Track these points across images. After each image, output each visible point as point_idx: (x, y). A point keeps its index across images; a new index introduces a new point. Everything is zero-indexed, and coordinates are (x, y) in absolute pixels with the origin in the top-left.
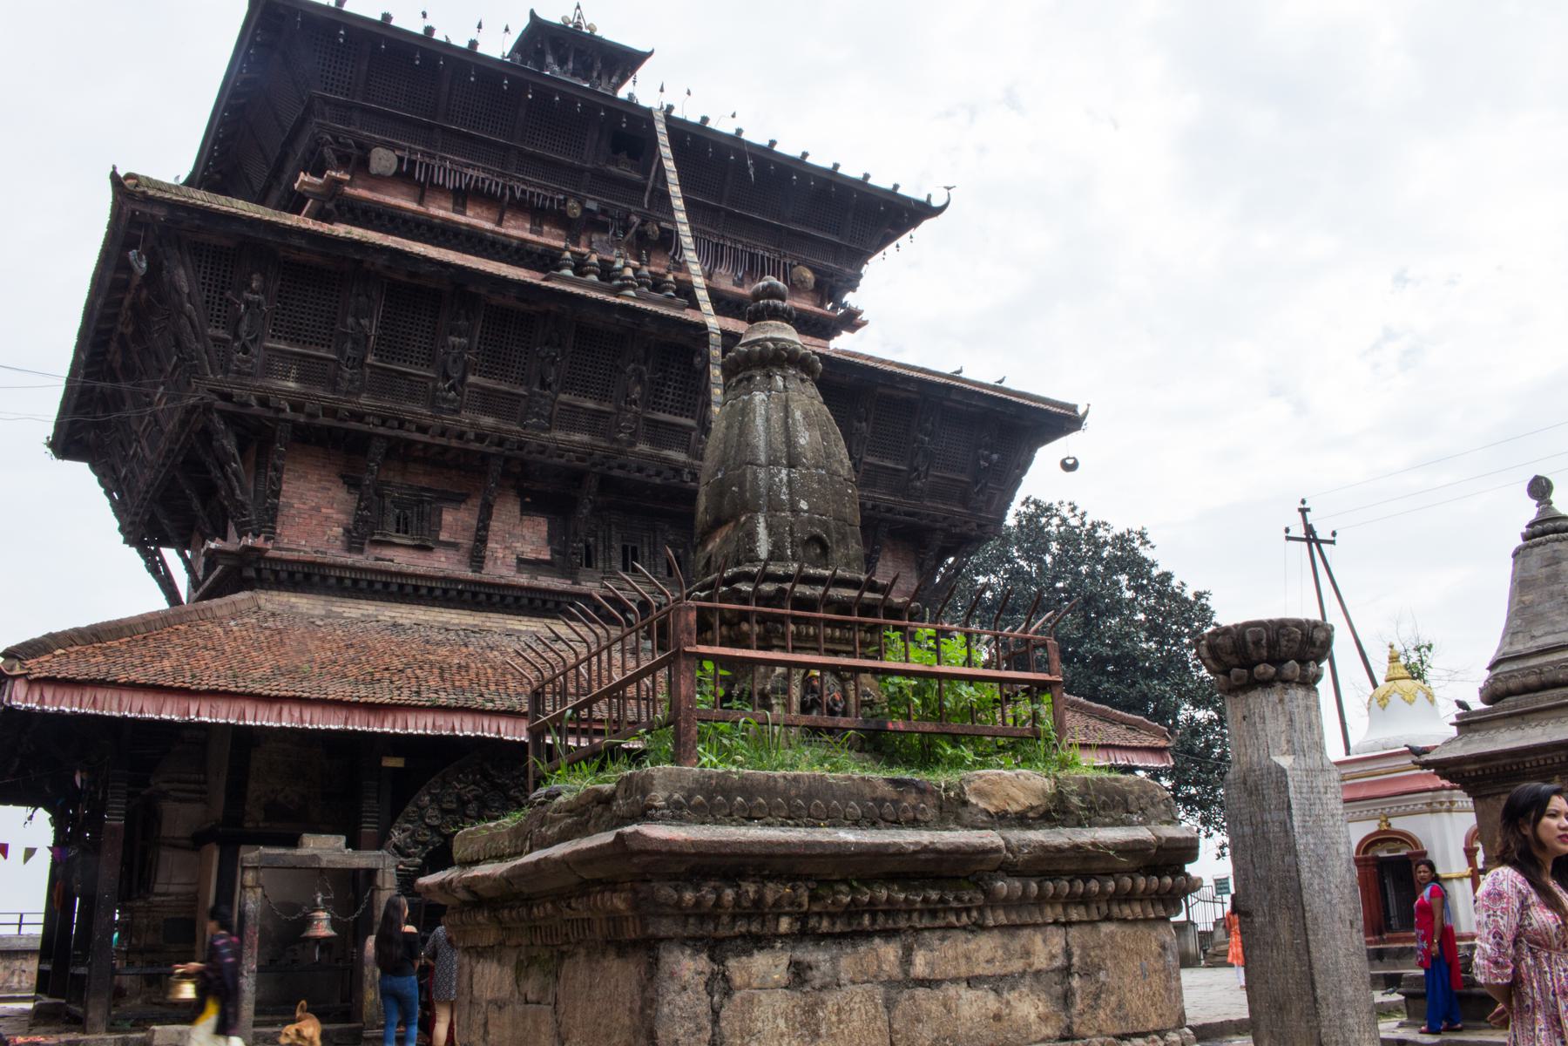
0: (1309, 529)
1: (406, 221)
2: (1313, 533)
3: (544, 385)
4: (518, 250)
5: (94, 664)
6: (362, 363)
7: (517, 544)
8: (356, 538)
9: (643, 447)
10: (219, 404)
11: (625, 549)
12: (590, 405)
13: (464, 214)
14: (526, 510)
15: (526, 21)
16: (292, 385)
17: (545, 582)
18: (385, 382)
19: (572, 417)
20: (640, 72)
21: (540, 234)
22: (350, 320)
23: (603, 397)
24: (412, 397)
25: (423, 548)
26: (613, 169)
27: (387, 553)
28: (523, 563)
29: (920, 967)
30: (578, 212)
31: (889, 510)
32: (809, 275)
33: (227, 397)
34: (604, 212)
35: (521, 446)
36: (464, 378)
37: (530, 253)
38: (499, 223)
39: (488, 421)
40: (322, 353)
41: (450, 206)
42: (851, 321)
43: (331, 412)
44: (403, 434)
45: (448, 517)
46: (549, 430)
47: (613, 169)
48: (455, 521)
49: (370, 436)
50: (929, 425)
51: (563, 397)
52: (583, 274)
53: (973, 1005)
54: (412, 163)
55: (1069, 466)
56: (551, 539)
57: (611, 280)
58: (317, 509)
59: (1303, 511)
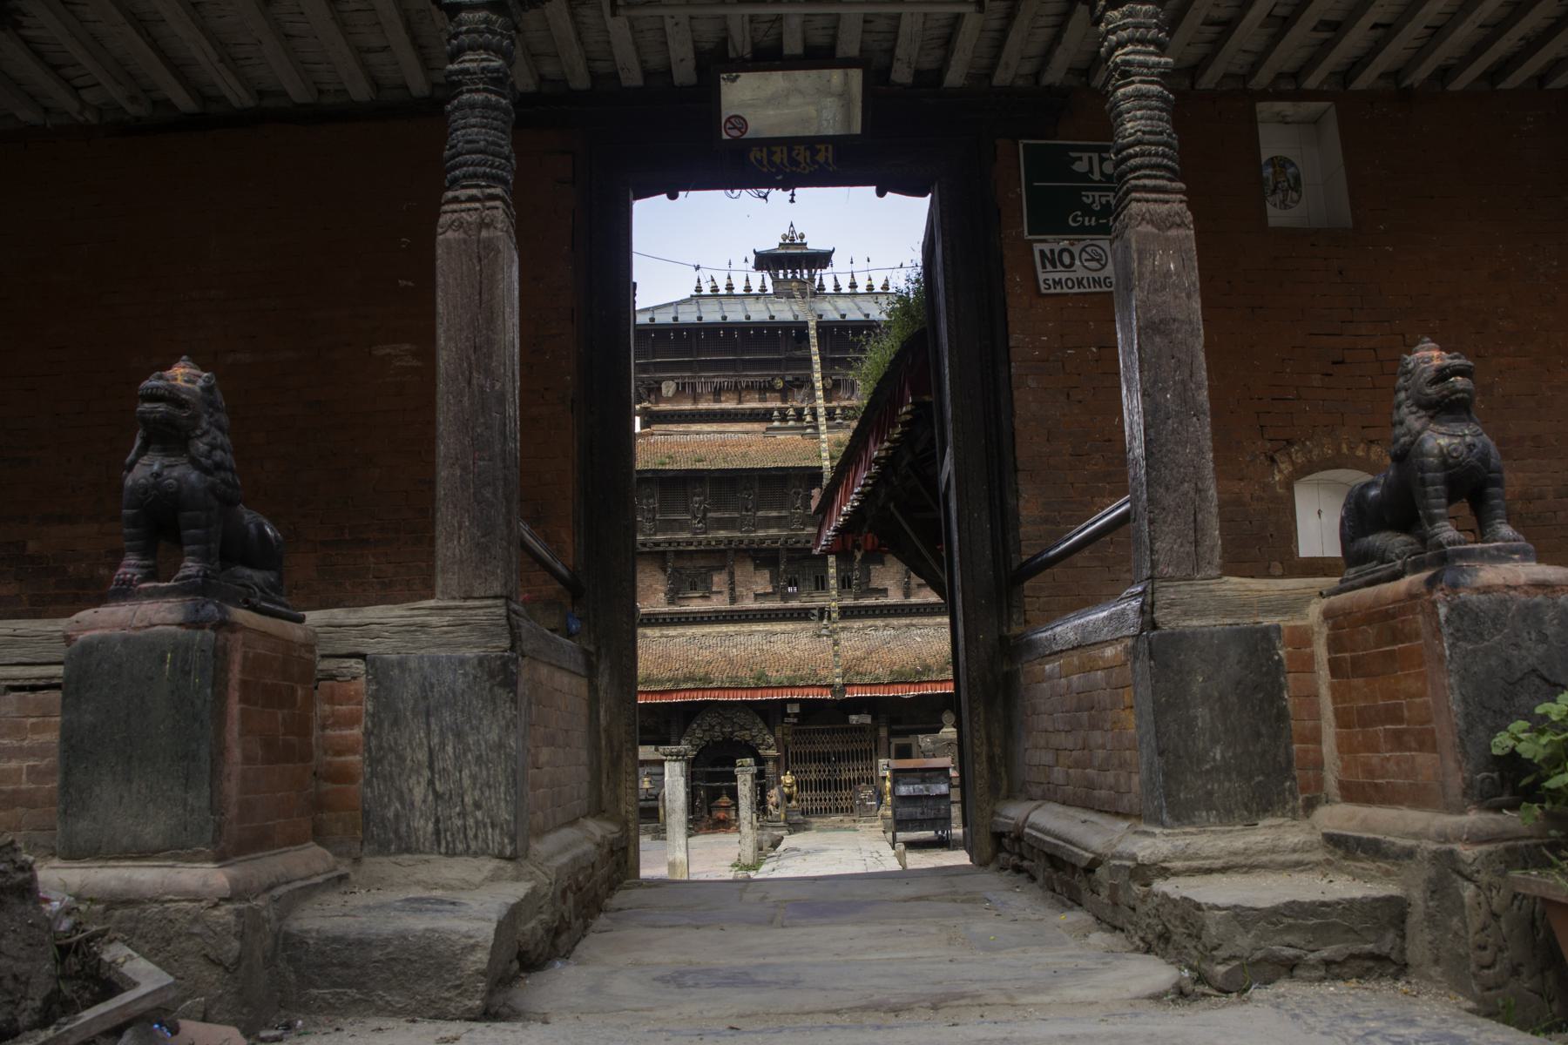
7: (755, 588)
12: (775, 514)
14: (757, 567)
17: (767, 605)
18: (669, 526)
19: (767, 523)
23: (782, 508)
24: (682, 529)
26: (798, 353)
28: (757, 596)
35: (741, 542)
39: (722, 534)
45: (716, 579)
48: (719, 580)
49: (664, 553)
51: (760, 514)
56: (774, 579)
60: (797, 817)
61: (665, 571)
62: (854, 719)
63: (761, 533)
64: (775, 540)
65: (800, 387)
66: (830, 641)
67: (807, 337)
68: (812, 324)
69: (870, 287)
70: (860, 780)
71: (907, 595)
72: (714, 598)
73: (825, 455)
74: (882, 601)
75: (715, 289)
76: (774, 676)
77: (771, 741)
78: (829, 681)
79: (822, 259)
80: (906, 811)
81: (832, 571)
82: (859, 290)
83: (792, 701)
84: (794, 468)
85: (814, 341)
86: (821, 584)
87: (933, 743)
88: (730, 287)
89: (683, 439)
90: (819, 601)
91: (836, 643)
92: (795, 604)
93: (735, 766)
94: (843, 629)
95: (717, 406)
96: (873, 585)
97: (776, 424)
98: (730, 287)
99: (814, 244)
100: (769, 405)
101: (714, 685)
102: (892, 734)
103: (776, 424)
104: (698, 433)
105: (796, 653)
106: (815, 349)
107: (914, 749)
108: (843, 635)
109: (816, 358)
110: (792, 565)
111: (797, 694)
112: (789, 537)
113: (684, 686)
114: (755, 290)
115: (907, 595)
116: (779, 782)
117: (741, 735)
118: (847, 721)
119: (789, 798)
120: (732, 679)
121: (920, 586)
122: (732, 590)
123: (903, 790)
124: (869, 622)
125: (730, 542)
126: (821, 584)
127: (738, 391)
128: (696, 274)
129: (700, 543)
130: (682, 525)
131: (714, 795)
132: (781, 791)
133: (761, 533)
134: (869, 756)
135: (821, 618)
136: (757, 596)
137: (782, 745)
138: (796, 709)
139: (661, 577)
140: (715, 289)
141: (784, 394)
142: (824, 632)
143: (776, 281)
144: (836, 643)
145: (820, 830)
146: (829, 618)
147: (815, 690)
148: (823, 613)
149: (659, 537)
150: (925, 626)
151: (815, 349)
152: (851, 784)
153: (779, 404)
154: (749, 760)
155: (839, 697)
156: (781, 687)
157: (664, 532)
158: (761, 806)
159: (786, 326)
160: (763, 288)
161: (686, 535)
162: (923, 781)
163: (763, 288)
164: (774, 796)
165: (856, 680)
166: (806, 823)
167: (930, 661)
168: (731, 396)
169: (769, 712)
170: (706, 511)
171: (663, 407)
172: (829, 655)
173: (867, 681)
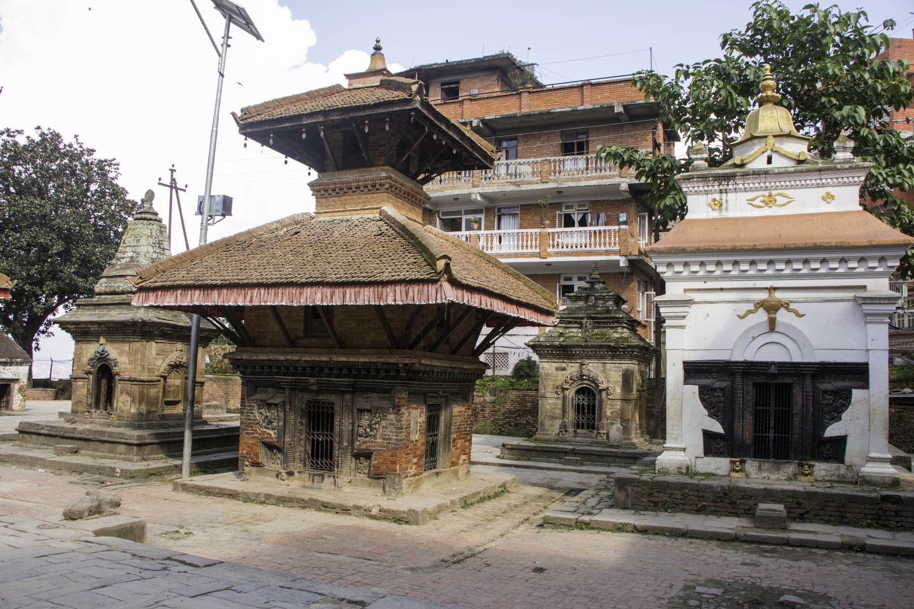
0: (173, 180)
2: (175, 183)
59: (172, 171)
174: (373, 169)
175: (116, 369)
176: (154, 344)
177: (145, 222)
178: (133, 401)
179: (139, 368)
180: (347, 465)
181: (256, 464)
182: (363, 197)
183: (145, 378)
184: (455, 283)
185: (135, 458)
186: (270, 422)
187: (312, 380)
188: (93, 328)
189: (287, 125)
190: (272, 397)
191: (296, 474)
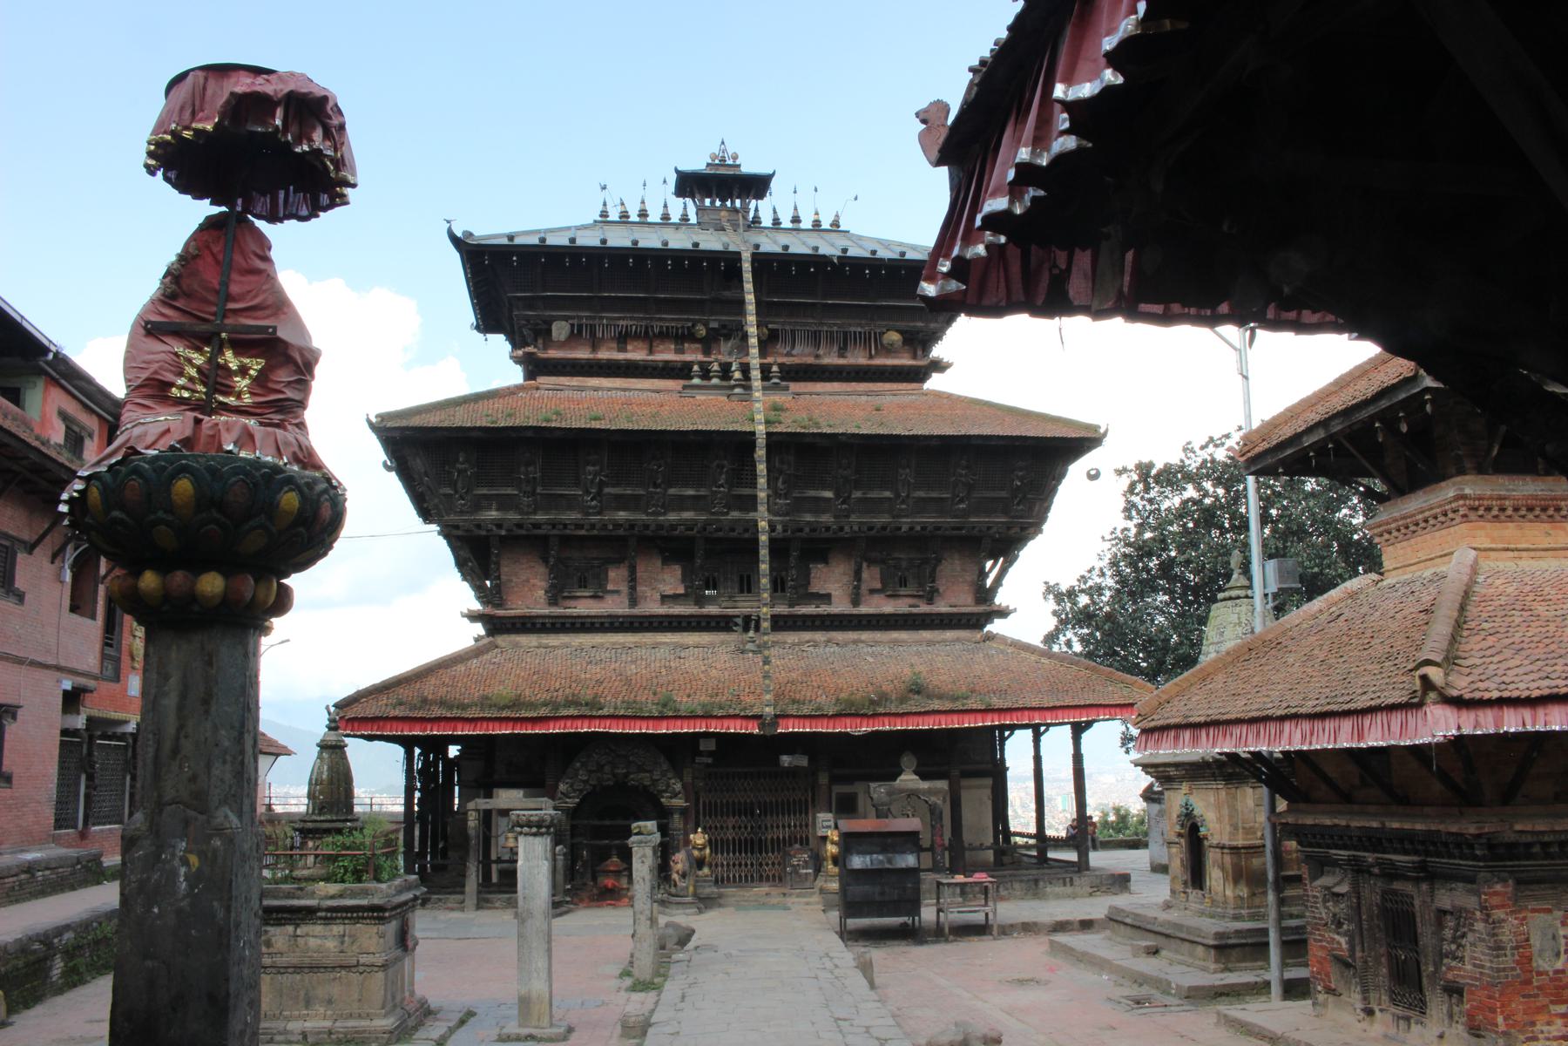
1: (582, 366)
3: (656, 486)
4: (663, 369)
5: (371, 709)
6: (533, 493)
7: (662, 586)
8: (554, 597)
9: (735, 514)
10: (456, 532)
11: (741, 578)
12: (691, 492)
13: (622, 349)
14: (666, 561)
15: (675, 176)
16: (494, 514)
18: (553, 502)
19: (681, 503)
20: (772, 184)
21: (680, 351)
22: (523, 469)
23: (699, 486)
24: (570, 508)
25: (594, 597)
26: (727, 294)
27: (572, 603)
28: (665, 599)
29: (299, 932)
30: (703, 332)
31: (938, 528)
32: (894, 337)
33: (457, 527)
34: (724, 327)
35: (646, 527)
36: (599, 493)
37: (673, 369)
38: (651, 352)
39: (622, 515)
40: (509, 491)
41: (614, 345)
42: (939, 366)
43: (519, 526)
44: (568, 532)
45: (612, 574)
46: (664, 514)
47: (727, 294)
48: (616, 577)
49: (546, 538)
50: (964, 462)
51: (672, 491)
52: (710, 379)
53: (313, 942)
54: (580, 327)
55: (1093, 476)
56: (683, 581)
57: (730, 378)
58: (528, 581)
60: (710, 890)
61: (545, 561)
62: (786, 760)
63: (672, 517)
64: (690, 525)
65: (727, 337)
66: (759, 659)
67: (740, 270)
68: (746, 256)
69: (817, 224)
70: (792, 840)
71: (856, 602)
72: (609, 599)
73: (759, 417)
74: (824, 609)
75: (624, 215)
76: (684, 703)
77: (678, 787)
78: (756, 711)
79: (757, 185)
80: (859, 890)
81: (764, 567)
82: (803, 226)
83: (706, 735)
84: (718, 432)
85: (748, 276)
86: (747, 585)
87: (889, 794)
88: (643, 214)
89: (576, 395)
90: (744, 607)
91: (766, 662)
92: (712, 610)
93: (629, 834)
94: (775, 643)
95: (621, 356)
96: (813, 589)
97: (696, 381)
98: (643, 214)
99: (749, 167)
100: (688, 357)
101: (605, 712)
102: (834, 780)
103: (696, 381)
104: (596, 389)
105: (714, 673)
106: (748, 286)
107: (862, 801)
108: (773, 652)
109: (750, 298)
110: (715, 559)
111: (715, 727)
112: (707, 523)
113: (565, 712)
114: (675, 218)
115: (856, 603)
116: (687, 842)
117: (636, 778)
118: (777, 762)
119: (700, 863)
120: (628, 705)
121: (872, 591)
122: (633, 588)
123: (857, 862)
124: (807, 635)
125: (632, 526)
126: (747, 585)
127: (649, 338)
128: (601, 196)
129: (593, 526)
130: (570, 503)
131: (601, 855)
132: (689, 855)
133: (672, 517)
134: (804, 808)
135: (746, 629)
136: (665, 599)
137: (690, 792)
138: (711, 745)
139: (542, 569)
140: (624, 215)
141: (708, 344)
142: (750, 646)
143: (700, 210)
144: (766, 662)
145: (739, 907)
146: (757, 629)
147: (738, 722)
148: (750, 623)
149: (540, 517)
150: (877, 643)
151: (748, 286)
152: (781, 846)
153: (700, 357)
154: (651, 825)
155: (769, 732)
156: (692, 717)
157: (547, 510)
158: (663, 870)
159: (713, 257)
160: (685, 218)
161: (575, 516)
162: (884, 850)
163: (685, 218)
164: (680, 861)
165: (792, 710)
166: (721, 896)
167: (887, 687)
168: (640, 344)
169: (677, 749)
170: (602, 485)
171: (553, 354)
172: (758, 677)
173: (806, 711)
174: (1443, 484)
175: (1203, 831)
176: (1249, 791)
177: (1229, 603)
178: (1225, 879)
179: (1228, 828)
180: (1437, 1005)
181: (1330, 991)
182: (1437, 534)
183: (1240, 842)
184: (1459, 703)
185: (1213, 966)
186: (1339, 924)
187: (1370, 857)
188: (1173, 772)
189: (1289, 452)
190: (1338, 884)
191: (1378, 1013)
